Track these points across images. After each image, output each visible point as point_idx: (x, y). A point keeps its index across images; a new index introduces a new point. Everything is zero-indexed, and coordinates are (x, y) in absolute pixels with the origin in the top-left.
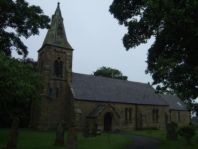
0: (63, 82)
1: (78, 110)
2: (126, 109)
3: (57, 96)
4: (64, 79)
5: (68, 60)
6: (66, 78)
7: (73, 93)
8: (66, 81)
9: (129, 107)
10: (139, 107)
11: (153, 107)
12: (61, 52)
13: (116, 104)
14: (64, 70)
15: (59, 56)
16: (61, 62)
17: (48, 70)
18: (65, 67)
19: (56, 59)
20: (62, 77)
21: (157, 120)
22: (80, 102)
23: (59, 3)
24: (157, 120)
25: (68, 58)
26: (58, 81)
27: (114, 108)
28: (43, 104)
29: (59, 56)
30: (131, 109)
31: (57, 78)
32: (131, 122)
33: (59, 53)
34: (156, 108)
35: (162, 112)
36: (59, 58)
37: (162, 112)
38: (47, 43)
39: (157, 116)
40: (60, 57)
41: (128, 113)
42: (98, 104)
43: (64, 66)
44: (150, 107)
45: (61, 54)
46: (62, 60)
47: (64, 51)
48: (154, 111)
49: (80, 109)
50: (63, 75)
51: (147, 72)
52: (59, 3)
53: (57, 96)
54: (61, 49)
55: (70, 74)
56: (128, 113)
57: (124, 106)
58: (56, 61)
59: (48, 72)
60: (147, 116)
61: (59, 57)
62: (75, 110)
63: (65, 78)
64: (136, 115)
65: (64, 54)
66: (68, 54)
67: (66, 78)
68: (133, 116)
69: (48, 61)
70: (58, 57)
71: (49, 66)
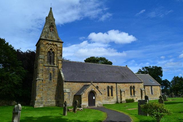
0: (55, 68)
1: (67, 90)
2: (108, 87)
3: (51, 80)
4: (56, 66)
5: (59, 50)
6: (57, 64)
7: (63, 76)
8: (58, 67)
9: (110, 85)
10: (119, 85)
11: (130, 84)
12: (53, 44)
13: (99, 84)
14: (55, 58)
15: (51, 48)
16: (53, 52)
17: (42, 59)
18: (57, 56)
19: (49, 50)
20: (54, 64)
21: (134, 95)
22: (68, 83)
23: (51, 8)
24: (134, 95)
25: (58, 49)
26: (50, 68)
27: (97, 87)
28: (39, 86)
29: (51, 48)
30: (112, 87)
31: (50, 65)
32: (109, 97)
33: (51, 45)
34: (132, 85)
35: (137, 88)
36: (51, 49)
37: (137, 88)
38: (42, 38)
39: (134, 91)
40: (52, 48)
41: (110, 90)
42: (85, 84)
43: (56, 55)
44: (128, 84)
45: (52, 46)
46: (53, 50)
47: (55, 43)
48: (131, 87)
49: (68, 89)
50: (55, 63)
51: (108, 34)
52: (51, 8)
53: (51, 80)
54: (53, 42)
55: (61, 61)
56: (110, 90)
57: (106, 85)
58: (49, 52)
59: (42, 60)
60: (126, 92)
61: (51, 49)
62: (64, 90)
63: (57, 65)
64: (117, 92)
65: (55, 46)
66: (58, 46)
67: (57, 64)
68: (114, 93)
69: (42, 51)
70: (50, 48)
71: (43, 56)
